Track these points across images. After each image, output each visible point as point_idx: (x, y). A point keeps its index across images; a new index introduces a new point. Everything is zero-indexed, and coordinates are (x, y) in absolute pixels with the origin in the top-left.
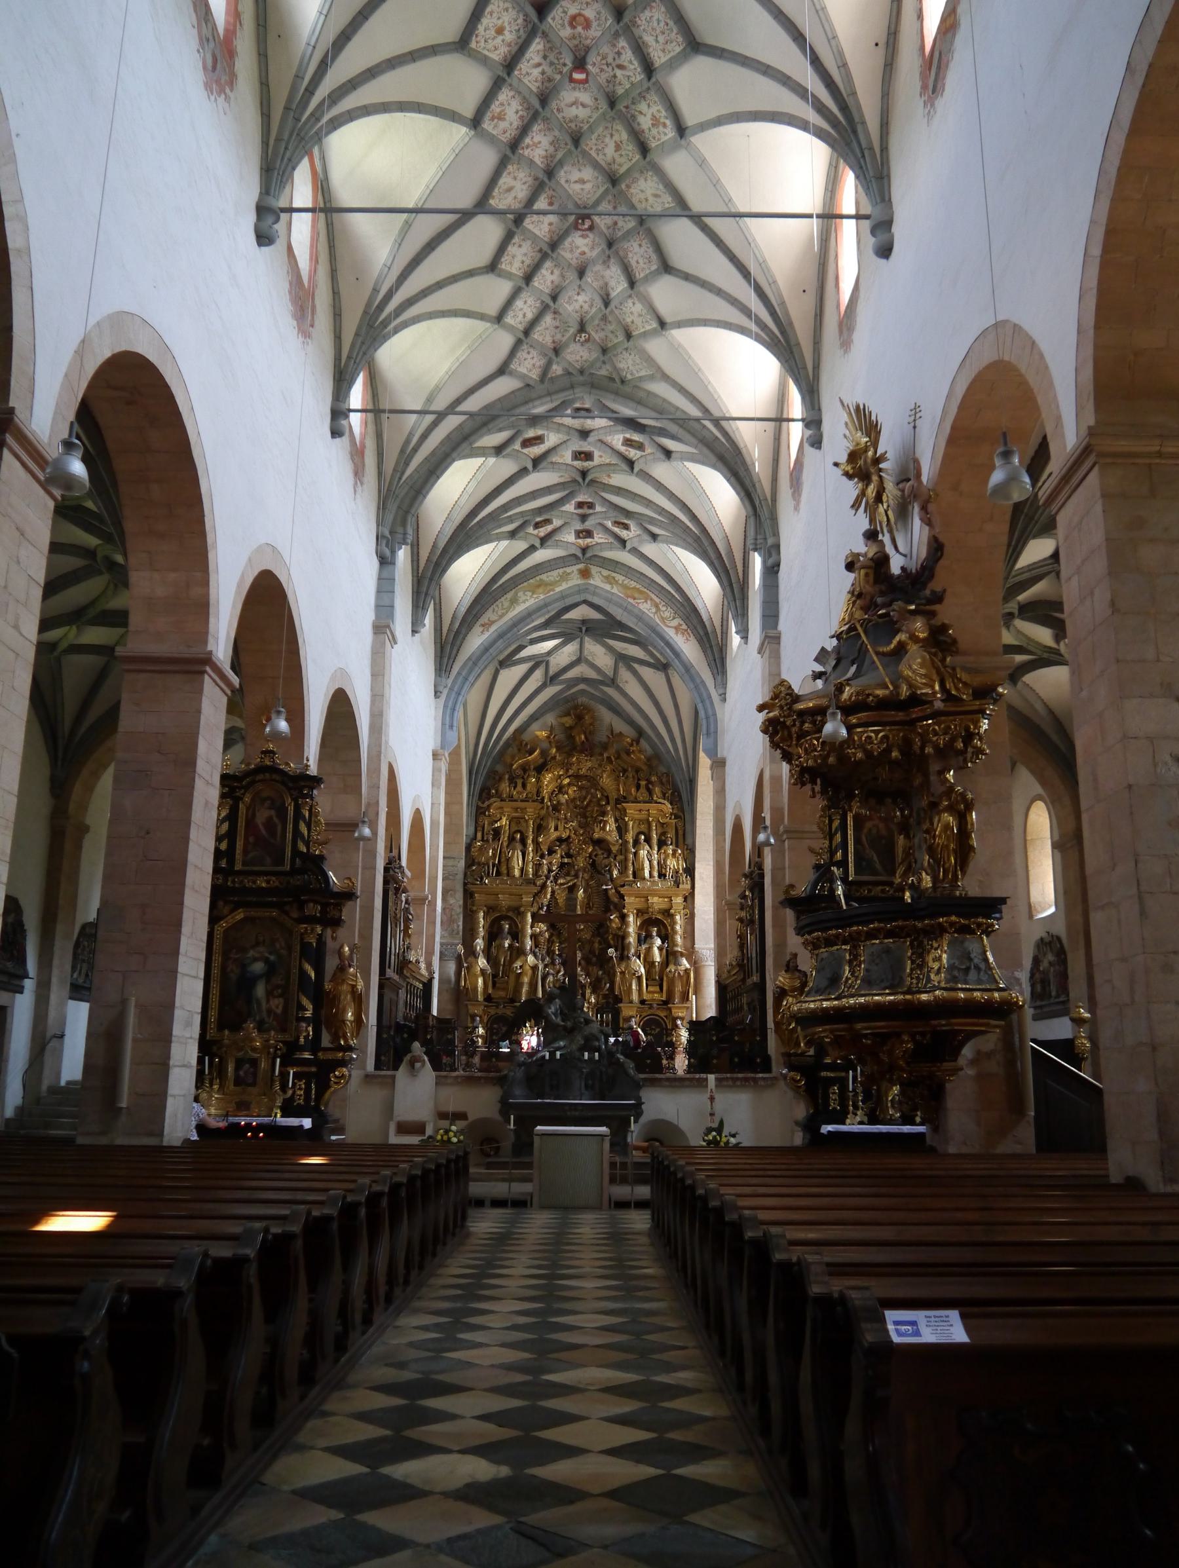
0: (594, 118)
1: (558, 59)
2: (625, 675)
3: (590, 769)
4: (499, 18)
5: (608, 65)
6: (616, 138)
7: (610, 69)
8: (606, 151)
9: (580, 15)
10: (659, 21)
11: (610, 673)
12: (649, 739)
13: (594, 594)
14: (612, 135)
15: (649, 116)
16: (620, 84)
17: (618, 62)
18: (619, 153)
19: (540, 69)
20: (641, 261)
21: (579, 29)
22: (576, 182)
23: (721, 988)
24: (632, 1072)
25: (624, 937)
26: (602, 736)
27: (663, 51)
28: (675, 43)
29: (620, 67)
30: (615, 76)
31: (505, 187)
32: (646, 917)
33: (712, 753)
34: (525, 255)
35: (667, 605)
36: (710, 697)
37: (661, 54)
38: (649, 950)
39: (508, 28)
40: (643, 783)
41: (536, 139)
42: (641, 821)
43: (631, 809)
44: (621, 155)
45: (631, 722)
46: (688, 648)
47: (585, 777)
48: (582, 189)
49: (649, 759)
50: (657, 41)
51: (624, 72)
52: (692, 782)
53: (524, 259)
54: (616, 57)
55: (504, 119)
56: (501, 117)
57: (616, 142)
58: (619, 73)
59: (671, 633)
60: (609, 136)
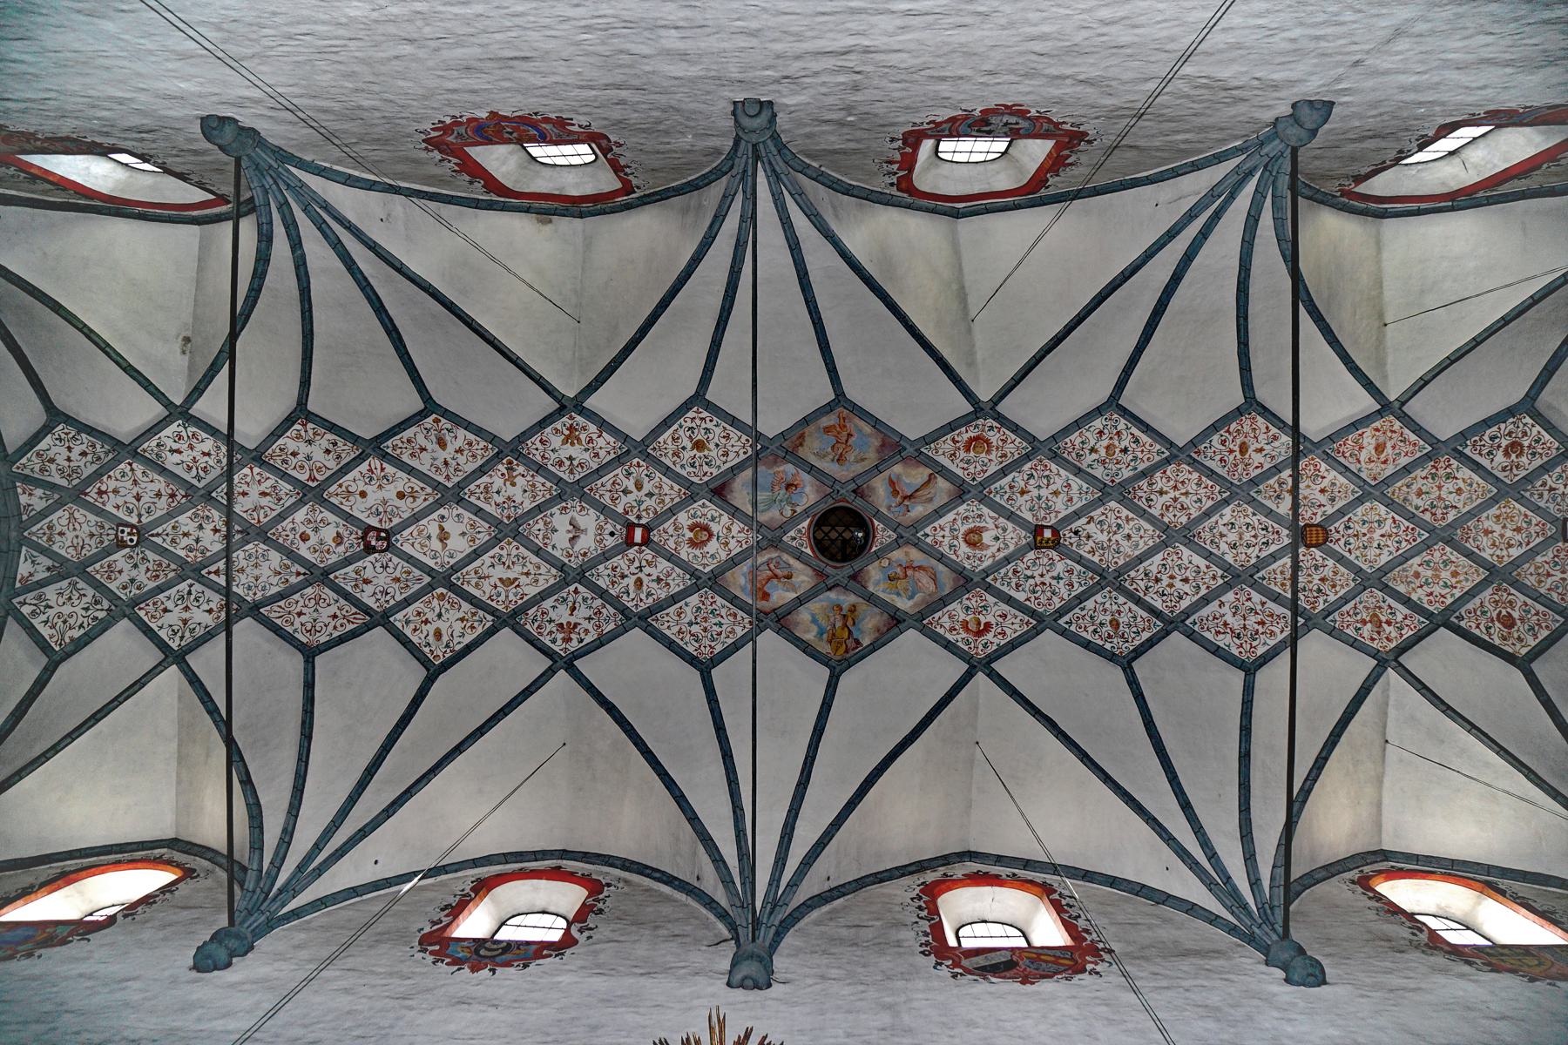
0: (554, 553)
1: (646, 510)
4: (717, 445)
5: (640, 568)
6: (523, 580)
7: (633, 569)
8: (499, 568)
9: (711, 535)
10: (720, 625)
14: (527, 574)
15: (573, 620)
16: (613, 583)
17: (646, 580)
18: (499, 584)
19: (632, 487)
20: (303, 619)
21: (690, 535)
22: (442, 529)
27: (680, 632)
28: (697, 645)
29: (639, 583)
30: (623, 576)
31: (448, 438)
34: (309, 458)
37: (675, 629)
39: (698, 454)
41: (520, 481)
44: (496, 587)
48: (429, 537)
50: (690, 624)
51: (632, 588)
53: (300, 457)
54: (654, 577)
55: (565, 442)
56: (571, 437)
57: (516, 579)
58: (631, 581)
60: (525, 570)
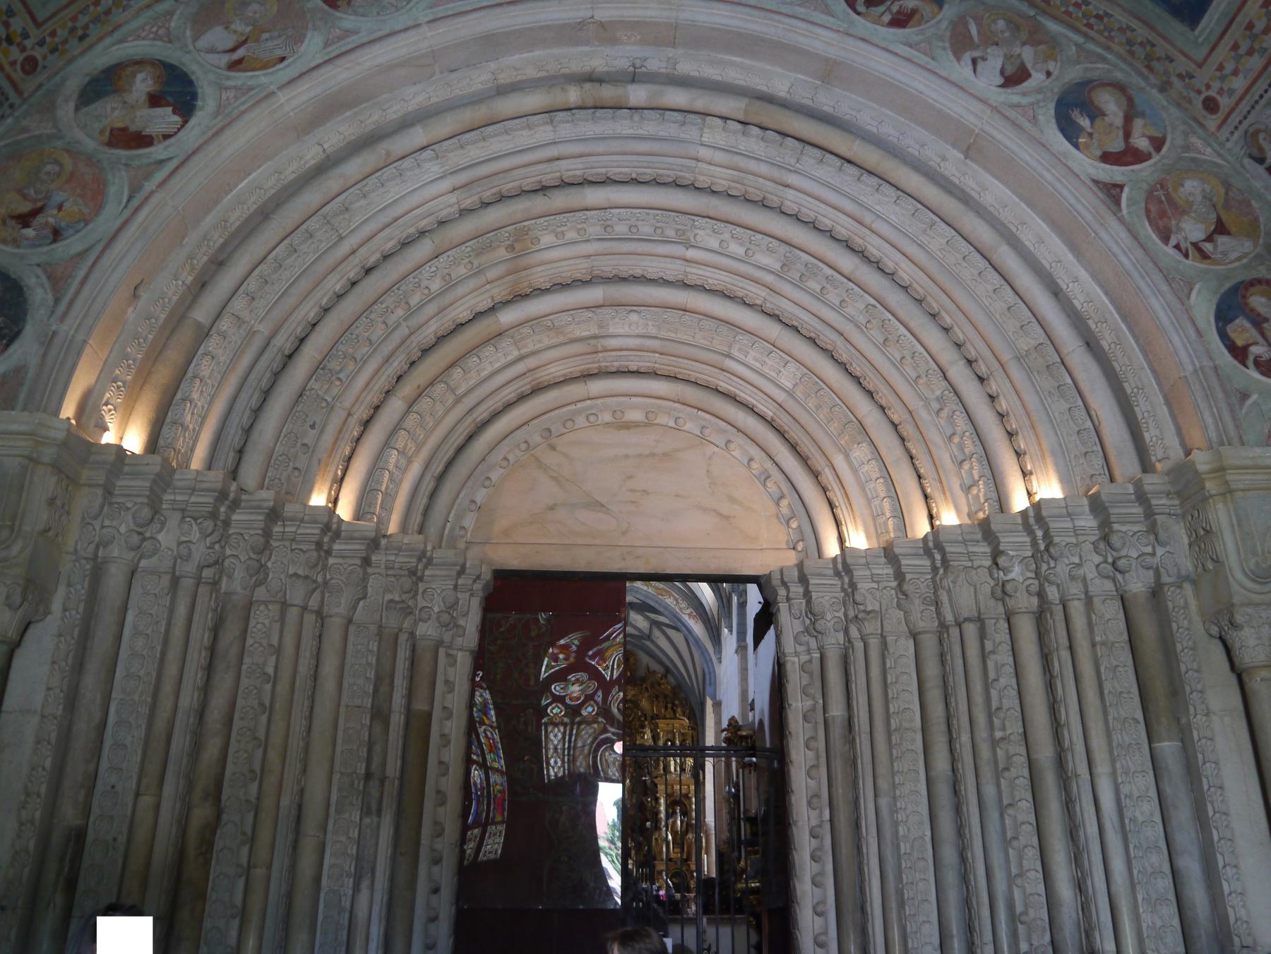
2: (656, 633)
3: (634, 696)
11: (647, 632)
12: (673, 674)
13: (637, 592)
23: (720, 856)
24: (662, 914)
25: (658, 813)
26: (641, 672)
32: (672, 799)
33: (714, 697)
35: (683, 600)
36: (711, 660)
38: (674, 823)
40: (669, 705)
42: (668, 732)
43: (662, 724)
45: (661, 662)
46: (697, 628)
47: (631, 701)
49: (673, 688)
52: (703, 705)
59: (686, 618)
